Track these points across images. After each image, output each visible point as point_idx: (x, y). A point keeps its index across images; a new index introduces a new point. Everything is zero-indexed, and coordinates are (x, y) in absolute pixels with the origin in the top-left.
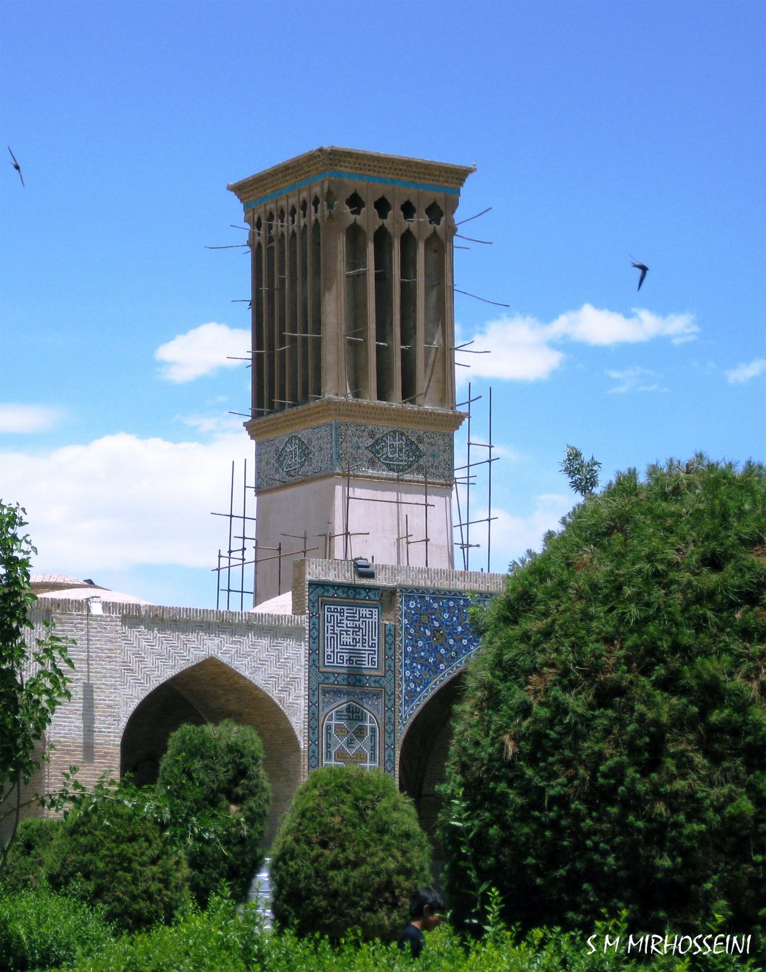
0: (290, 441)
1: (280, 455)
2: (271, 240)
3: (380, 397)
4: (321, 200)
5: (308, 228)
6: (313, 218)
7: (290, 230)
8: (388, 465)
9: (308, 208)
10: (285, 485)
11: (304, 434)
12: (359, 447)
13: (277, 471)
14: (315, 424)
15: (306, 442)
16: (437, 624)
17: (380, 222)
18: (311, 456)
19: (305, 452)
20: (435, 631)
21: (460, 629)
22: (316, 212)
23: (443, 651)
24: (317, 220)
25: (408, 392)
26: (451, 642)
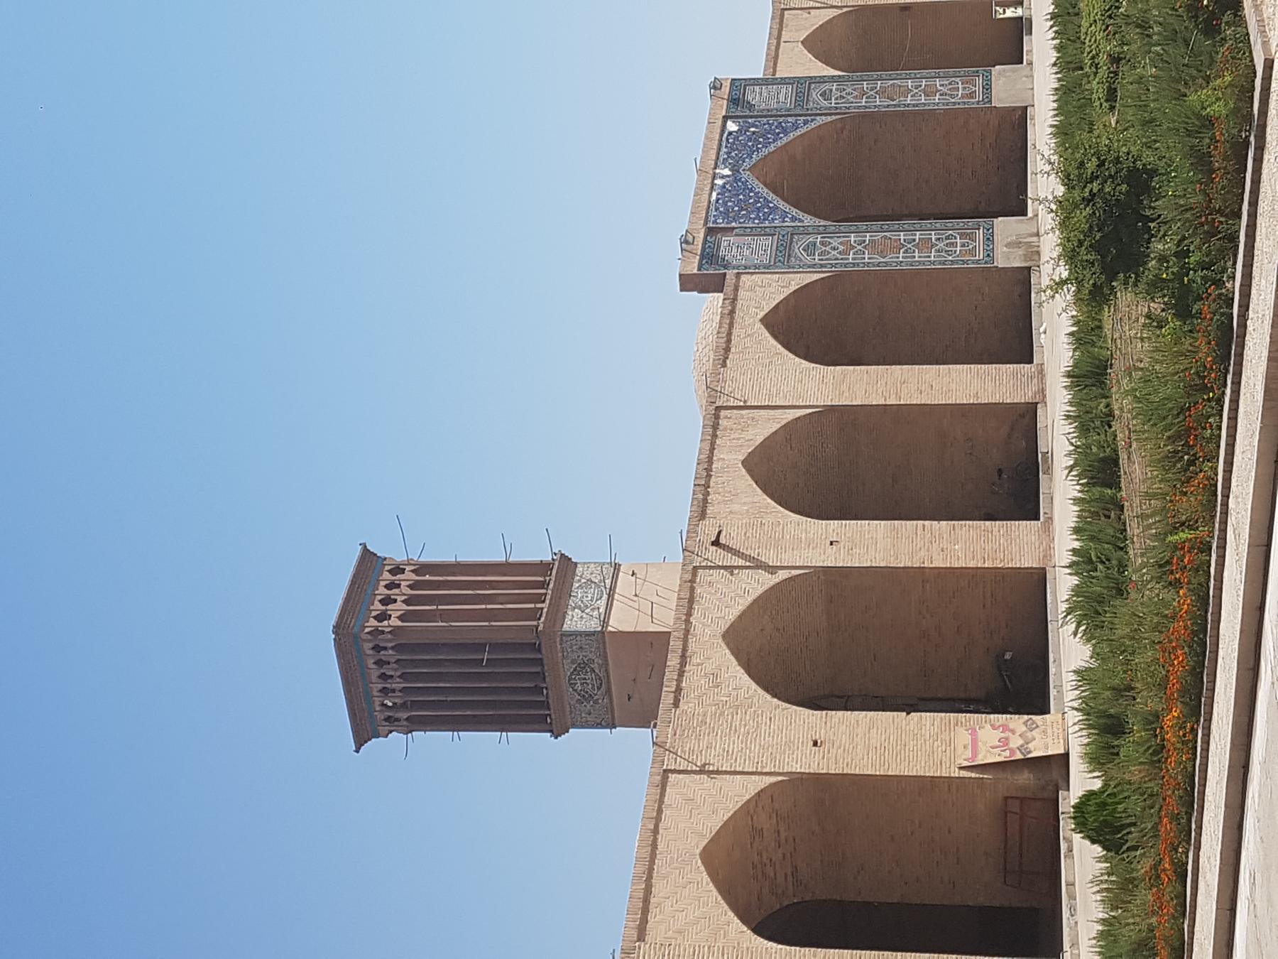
0: (572, 685)
1: (585, 697)
2: (404, 706)
3: (544, 602)
4: (377, 643)
5: (400, 657)
6: (391, 652)
7: (398, 680)
8: (597, 600)
9: (383, 658)
10: (609, 691)
11: (569, 668)
12: (581, 617)
13: (596, 702)
14: (560, 654)
15: (574, 666)
16: (736, 208)
17: (399, 603)
18: (585, 660)
19: (582, 667)
20: (742, 209)
21: (741, 197)
22: (385, 648)
23: (759, 205)
24: (392, 648)
25: (544, 585)
26: (751, 201)
